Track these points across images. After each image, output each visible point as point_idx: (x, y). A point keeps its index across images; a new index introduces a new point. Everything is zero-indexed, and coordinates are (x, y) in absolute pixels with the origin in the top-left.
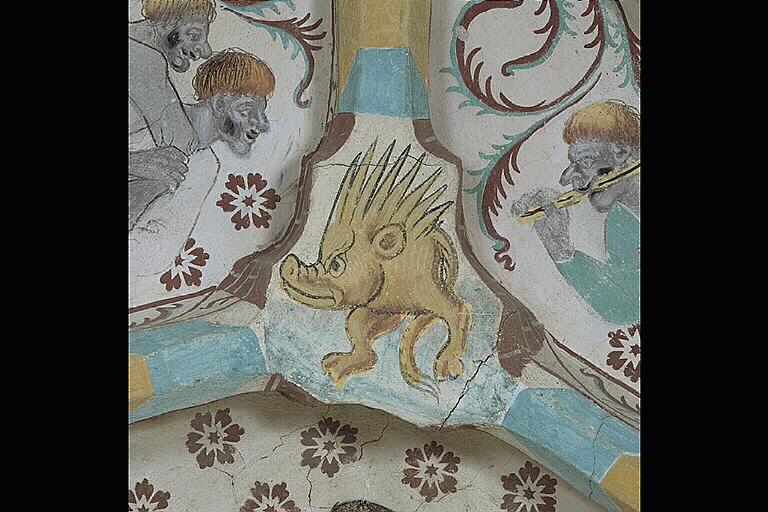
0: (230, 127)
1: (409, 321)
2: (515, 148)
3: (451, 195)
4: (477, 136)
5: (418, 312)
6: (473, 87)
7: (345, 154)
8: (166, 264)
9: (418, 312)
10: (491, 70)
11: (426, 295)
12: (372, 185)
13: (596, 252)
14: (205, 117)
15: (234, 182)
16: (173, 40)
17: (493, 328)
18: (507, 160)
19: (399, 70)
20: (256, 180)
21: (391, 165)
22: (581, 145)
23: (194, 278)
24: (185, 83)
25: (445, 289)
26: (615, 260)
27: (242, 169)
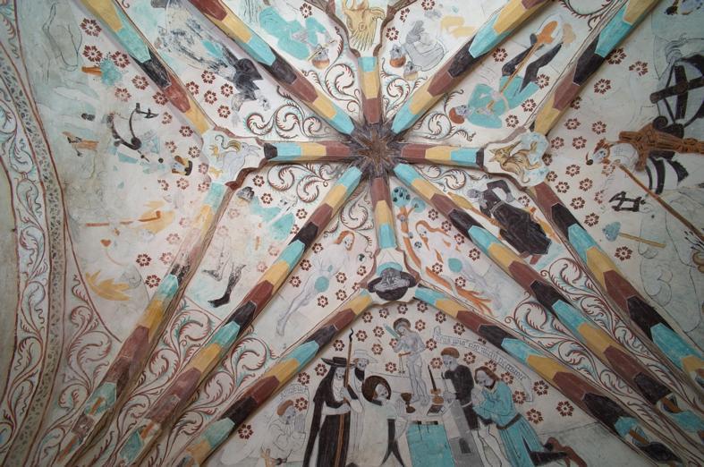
0: (398, 51)
1: (356, 8)
2: (339, 55)
3: (351, 41)
4: (345, 59)
5: (353, 10)
6: (349, 68)
7: (374, 46)
8: (408, 14)
9: (353, 10)
10: (347, 72)
11: (353, 15)
12: (367, 40)
13: (318, 33)
14: (403, 52)
15: (396, 38)
16: (411, 68)
17: (336, 7)
18: (340, 53)
19: (365, 68)
20: (391, 39)
21: (364, 45)
22: (326, 59)
23: (403, 12)
24: (408, 59)
25: (349, 17)
26: (314, 33)
27: (394, 41)
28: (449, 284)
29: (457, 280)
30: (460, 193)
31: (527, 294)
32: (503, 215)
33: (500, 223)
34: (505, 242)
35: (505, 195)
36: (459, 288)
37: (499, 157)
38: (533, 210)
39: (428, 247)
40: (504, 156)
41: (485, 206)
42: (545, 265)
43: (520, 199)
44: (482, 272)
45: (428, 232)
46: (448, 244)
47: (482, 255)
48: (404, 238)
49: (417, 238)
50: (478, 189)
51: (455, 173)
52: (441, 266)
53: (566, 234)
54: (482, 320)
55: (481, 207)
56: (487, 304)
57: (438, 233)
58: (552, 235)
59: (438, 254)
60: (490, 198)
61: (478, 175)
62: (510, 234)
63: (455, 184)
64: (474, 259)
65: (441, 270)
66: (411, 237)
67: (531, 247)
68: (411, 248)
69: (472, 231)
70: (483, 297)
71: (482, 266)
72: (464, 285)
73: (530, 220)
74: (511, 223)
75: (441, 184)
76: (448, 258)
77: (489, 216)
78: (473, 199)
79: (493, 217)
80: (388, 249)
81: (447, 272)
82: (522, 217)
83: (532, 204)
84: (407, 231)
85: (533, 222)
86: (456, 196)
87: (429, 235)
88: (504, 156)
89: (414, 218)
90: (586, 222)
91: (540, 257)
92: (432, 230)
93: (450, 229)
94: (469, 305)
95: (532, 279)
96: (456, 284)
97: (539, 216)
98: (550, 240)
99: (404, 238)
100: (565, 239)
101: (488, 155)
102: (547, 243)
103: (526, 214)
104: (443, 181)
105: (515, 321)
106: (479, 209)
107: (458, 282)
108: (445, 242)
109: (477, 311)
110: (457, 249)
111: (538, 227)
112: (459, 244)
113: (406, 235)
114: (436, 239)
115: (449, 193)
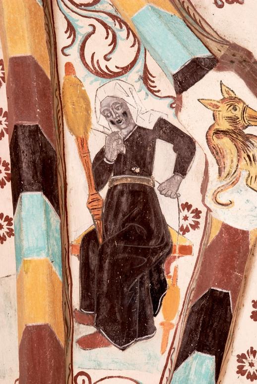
30: (91, 84)
32: (124, 207)
33: (105, 219)
34: (75, 264)
35: (170, 173)
37: (225, 111)
38: (186, 250)
40: (233, 120)
41: (111, 157)
42: (99, 366)
43: (187, 206)
50: (133, 111)
51: (122, 34)
53: (183, 356)
55: (102, 153)
58: (166, 325)
60: (138, 149)
61: (167, 87)
63: (99, 57)
67: (111, 312)
69: (33, 200)
73: (161, 262)
74: (124, 236)
75: (71, 29)
77: (99, 185)
78: (105, 122)
79: (103, 193)
82: (153, 243)
83: (194, 238)
85: (160, 271)
86: (79, 84)
88: (233, 120)
90: (241, 358)
91: (107, 345)
97: (183, 273)
98: (155, 329)
100: (174, 357)
101: (210, 85)
102: (144, 330)
103: (165, 246)
104: (83, 26)
106: (94, 152)
111: (159, 288)
115: (69, 66)
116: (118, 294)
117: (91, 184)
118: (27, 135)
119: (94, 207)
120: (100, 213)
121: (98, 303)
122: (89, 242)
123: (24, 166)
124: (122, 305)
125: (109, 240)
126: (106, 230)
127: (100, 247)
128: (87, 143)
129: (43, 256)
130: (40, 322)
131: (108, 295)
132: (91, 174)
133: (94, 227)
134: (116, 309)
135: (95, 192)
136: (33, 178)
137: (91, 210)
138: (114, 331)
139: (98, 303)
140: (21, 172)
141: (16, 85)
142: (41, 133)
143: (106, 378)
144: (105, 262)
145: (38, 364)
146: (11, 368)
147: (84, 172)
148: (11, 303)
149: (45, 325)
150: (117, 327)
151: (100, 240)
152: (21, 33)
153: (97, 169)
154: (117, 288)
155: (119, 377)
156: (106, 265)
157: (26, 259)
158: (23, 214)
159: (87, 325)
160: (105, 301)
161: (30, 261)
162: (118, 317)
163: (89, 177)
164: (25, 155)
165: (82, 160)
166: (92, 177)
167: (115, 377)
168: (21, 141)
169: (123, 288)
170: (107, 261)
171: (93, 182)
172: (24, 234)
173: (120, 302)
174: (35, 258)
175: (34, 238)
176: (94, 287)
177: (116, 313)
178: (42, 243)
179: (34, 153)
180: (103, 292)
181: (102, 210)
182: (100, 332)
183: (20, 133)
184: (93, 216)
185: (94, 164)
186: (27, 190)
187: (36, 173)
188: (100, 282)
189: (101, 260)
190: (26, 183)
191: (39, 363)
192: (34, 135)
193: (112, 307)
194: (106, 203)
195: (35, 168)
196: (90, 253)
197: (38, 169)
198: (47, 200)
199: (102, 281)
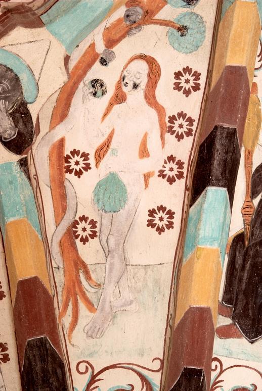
28: (64, 210)
29: (84, 218)
31: (157, 365)
33: (253, 224)
36: (71, 233)
39: (108, 110)
42: (230, 355)
44: (135, 258)
45: (140, 93)
46: (144, 152)
47: (172, 235)
48: (92, 46)
49: (109, 75)
52: (87, 167)
54: (53, 330)
56: (82, 306)
57: (153, 113)
59: (107, 144)
62: (246, 254)
64: (151, 224)
65: (79, 174)
66: (104, 62)
67: (246, 308)
68: (81, 78)
70: (90, 292)
71: (156, 250)
72: (84, 240)
76: (114, 169)
77: (253, 195)
79: (256, 201)
80: (55, 43)
81: (83, 188)
84: (111, 43)
87: (136, 98)
89: (150, 39)
91: (239, 337)
92: (150, 98)
93: (180, 137)
94: (58, 282)
95: (201, 364)
96: (76, 222)
99: (92, 46)
105: (93, 380)
107: (82, 225)
108: (144, 144)
109: (58, 303)
110: (147, 177)
112: (162, 175)
113: (100, 48)
114: (136, 120)
116: (253, 293)
117: (248, 192)
118: (224, 135)
119: (247, 213)
120: (250, 219)
121: (236, 301)
122: (237, 243)
123: (216, 163)
124: (255, 303)
125: (253, 244)
126: (252, 234)
127: (245, 249)
128: (252, 156)
129: (215, 246)
130: (204, 305)
131: (245, 293)
132: (250, 183)
133: (243, 230)
134: (250, 306)
135: (250, 199)
136: (222, 174)
137: (244, 215)
138: (246, 325)
139: (236, 301)
140: (212, 168)
141: (226, 90)
142: (236, 136)
143: (235, 366)
144: (247, 263)
145: (196, 342)
146: (150, 348)
147: (245, 180)
148: (160, 288)
149: (207, 308)
150: (249, 322)
151: (247, 243)
152: (242, 46)
153: (255, 180)
154: (253, 287)
155: (246, 367)
156: (248, 266)
157: (200, 246)
158: (205, 206)
159: (225, 316)
160: (242, 298)
161: (203, 248)
162: (251, 314)
163: (248, 186)
164: (218, 153)
165: (246, 170)
166: (250, 186)
167: (243, 366)
168: (218, 141)
169: (257, 288)
170: (249, 262)
171: (250, 191)
172: (202, 223)
173: (253, 301)
174: (209, 247)
175: (211, 229)
176: (236, 283)
177: (249, 309)
178: (216, 234)
179: (226, 153)
180: (242, 289)
181: (252, 217)
182: (235, 324)
183: (218, 133)
184: (244, 220)
185: (254, 175)
186: (213, 185)
187: (225, 171)
188: (241, 279)
189: (245, 261)
190: (214, 178)
191: (198, 342)
192: (231, 137)
193: (247, 304)
194: (257, 211)
195: (225, 166)
196: (237, 253)
197: (227, 167)
198: (228, 196)
199: (243, 279)
